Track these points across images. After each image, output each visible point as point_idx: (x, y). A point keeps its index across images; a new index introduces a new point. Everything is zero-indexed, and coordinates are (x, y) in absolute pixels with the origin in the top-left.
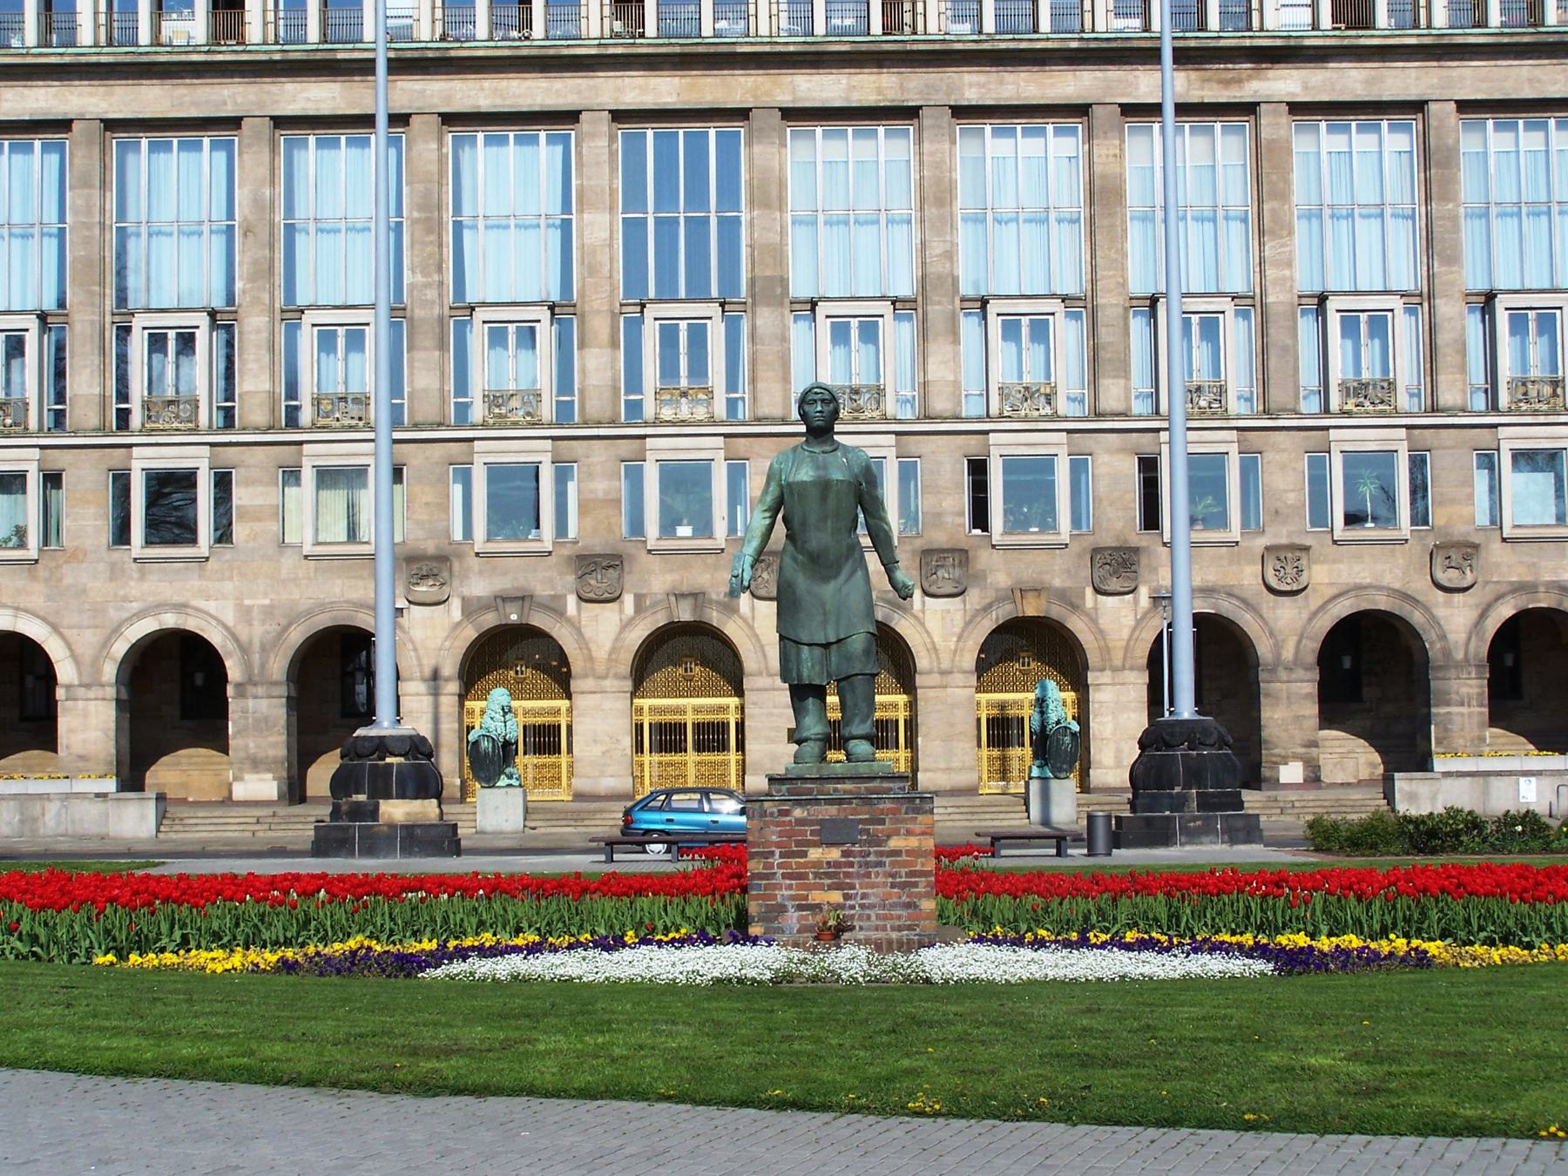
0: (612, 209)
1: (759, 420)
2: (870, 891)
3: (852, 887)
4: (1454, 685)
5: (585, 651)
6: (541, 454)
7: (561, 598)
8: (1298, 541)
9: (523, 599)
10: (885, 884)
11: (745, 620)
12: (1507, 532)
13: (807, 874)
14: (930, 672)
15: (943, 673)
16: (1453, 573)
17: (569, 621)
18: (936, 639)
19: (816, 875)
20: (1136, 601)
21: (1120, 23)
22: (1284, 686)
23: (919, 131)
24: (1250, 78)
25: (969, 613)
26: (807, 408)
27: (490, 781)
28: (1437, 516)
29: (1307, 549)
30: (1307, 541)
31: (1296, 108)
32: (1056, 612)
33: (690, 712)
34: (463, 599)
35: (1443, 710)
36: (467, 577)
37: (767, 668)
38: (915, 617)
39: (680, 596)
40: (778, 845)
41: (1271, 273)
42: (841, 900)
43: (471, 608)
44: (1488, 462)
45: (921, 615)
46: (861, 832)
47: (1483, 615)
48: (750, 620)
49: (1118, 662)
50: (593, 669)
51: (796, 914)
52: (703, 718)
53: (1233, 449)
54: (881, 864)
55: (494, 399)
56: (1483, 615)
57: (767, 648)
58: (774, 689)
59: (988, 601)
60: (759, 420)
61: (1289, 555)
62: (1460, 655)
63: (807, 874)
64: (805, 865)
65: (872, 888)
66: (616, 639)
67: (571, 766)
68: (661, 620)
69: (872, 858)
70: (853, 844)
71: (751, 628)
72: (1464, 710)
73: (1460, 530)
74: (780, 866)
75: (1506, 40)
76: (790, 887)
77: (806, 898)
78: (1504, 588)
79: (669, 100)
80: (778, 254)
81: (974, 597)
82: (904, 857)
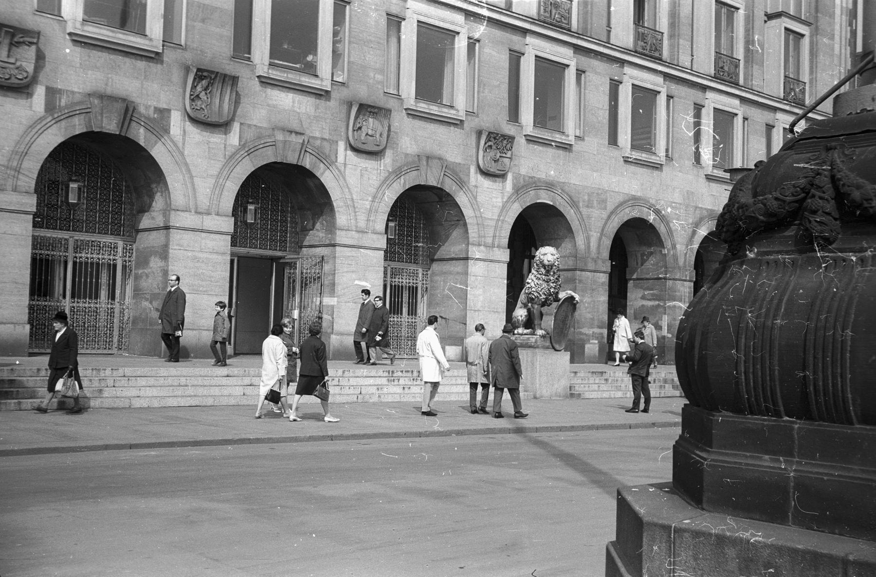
20: (504, 188)
32: (449, 186)
48: (180, 145)
49: (489, 240)
53: (573, 64)
58: (202, 231)
68: (78, 126)
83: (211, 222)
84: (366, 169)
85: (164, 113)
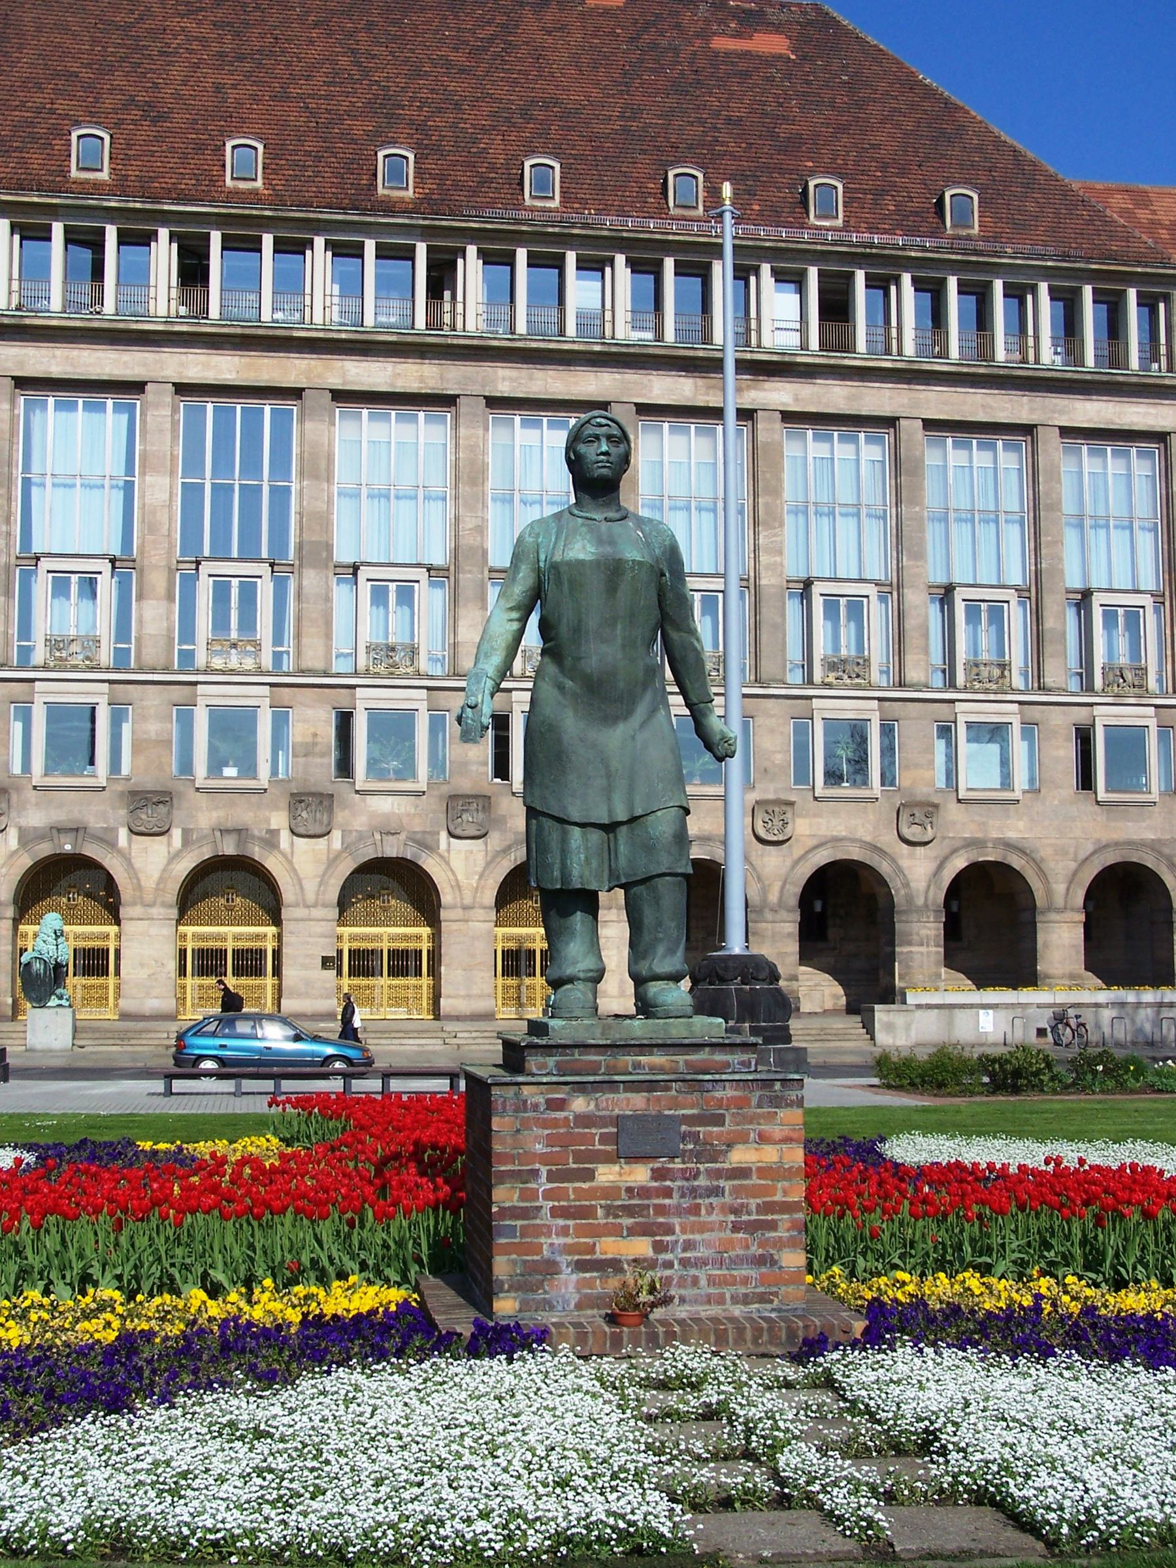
0: (172, 473)
1: (302, 672)
2: (697, 1237)
3: (670, 1230)
4: (915, 927)
5: (135, 881)
6: (99, 696)
7: (114, 831)
8: (783, 796)
9: (77, 830)
10: (722, 1225)
11: (284, 855)
12: (962, 794)
13: (594, 1207)
14: (453, 907)
15: (465, 908)
16: (916, 829)
17: (120, 852)
18: (459, 877)
19: (609, 1211)
21: (636, 336)
22: (770, 926)
23: (456, 418)
24: (749, 388)
25: (490, 854)
26: (582, 448)
27: (40, 1001)
28: (904, 778)
29: (791, 804)
30: (793, 799)
31: (788, 417)
33: (230, 940)
34: (20, 828)
35: (906, 949)
36: (25, 809)
37: (304, 900)
38: (441, 856)
39: (224, 832)
40: (545, 1159)
41: (764, 558)
42: (650, 1253)
43: (27, 838)
44: (946, 731)
45: (446, 854)
46: (684, 1137)
47: (940, 867)
48: (289, 856)
50: (141, 898)
51: (574, 1277)
52: (241, 945)
54: (717, 1191)
55: (55, 644)
56: (940, 867)
57: (304, 882)
58: (310, 920)
59: (507, 843)
60: (302, 672)
61: (777, 809)
62: (920, 901)
63: (594, 1207)
64: (592, 1193)
65: (701, 1232)
66: (164, 870)
67: (118, 987)
68: (206, 853)
69: (702, 1182)
70: (672, 1158)
71: (290, 862)
72: (923, 949)
73: (922, 792)
74: (548, 1195)
75: (965, 370)
76: (564, 1231)
77: (591, 1249)
78: (959, 844)
79: (228, 376)
80: (324, 521)
81: (495, 840)
82: (755, 1180)
83: (317, 913)
84: (471, 852)
85: (274, 833)
